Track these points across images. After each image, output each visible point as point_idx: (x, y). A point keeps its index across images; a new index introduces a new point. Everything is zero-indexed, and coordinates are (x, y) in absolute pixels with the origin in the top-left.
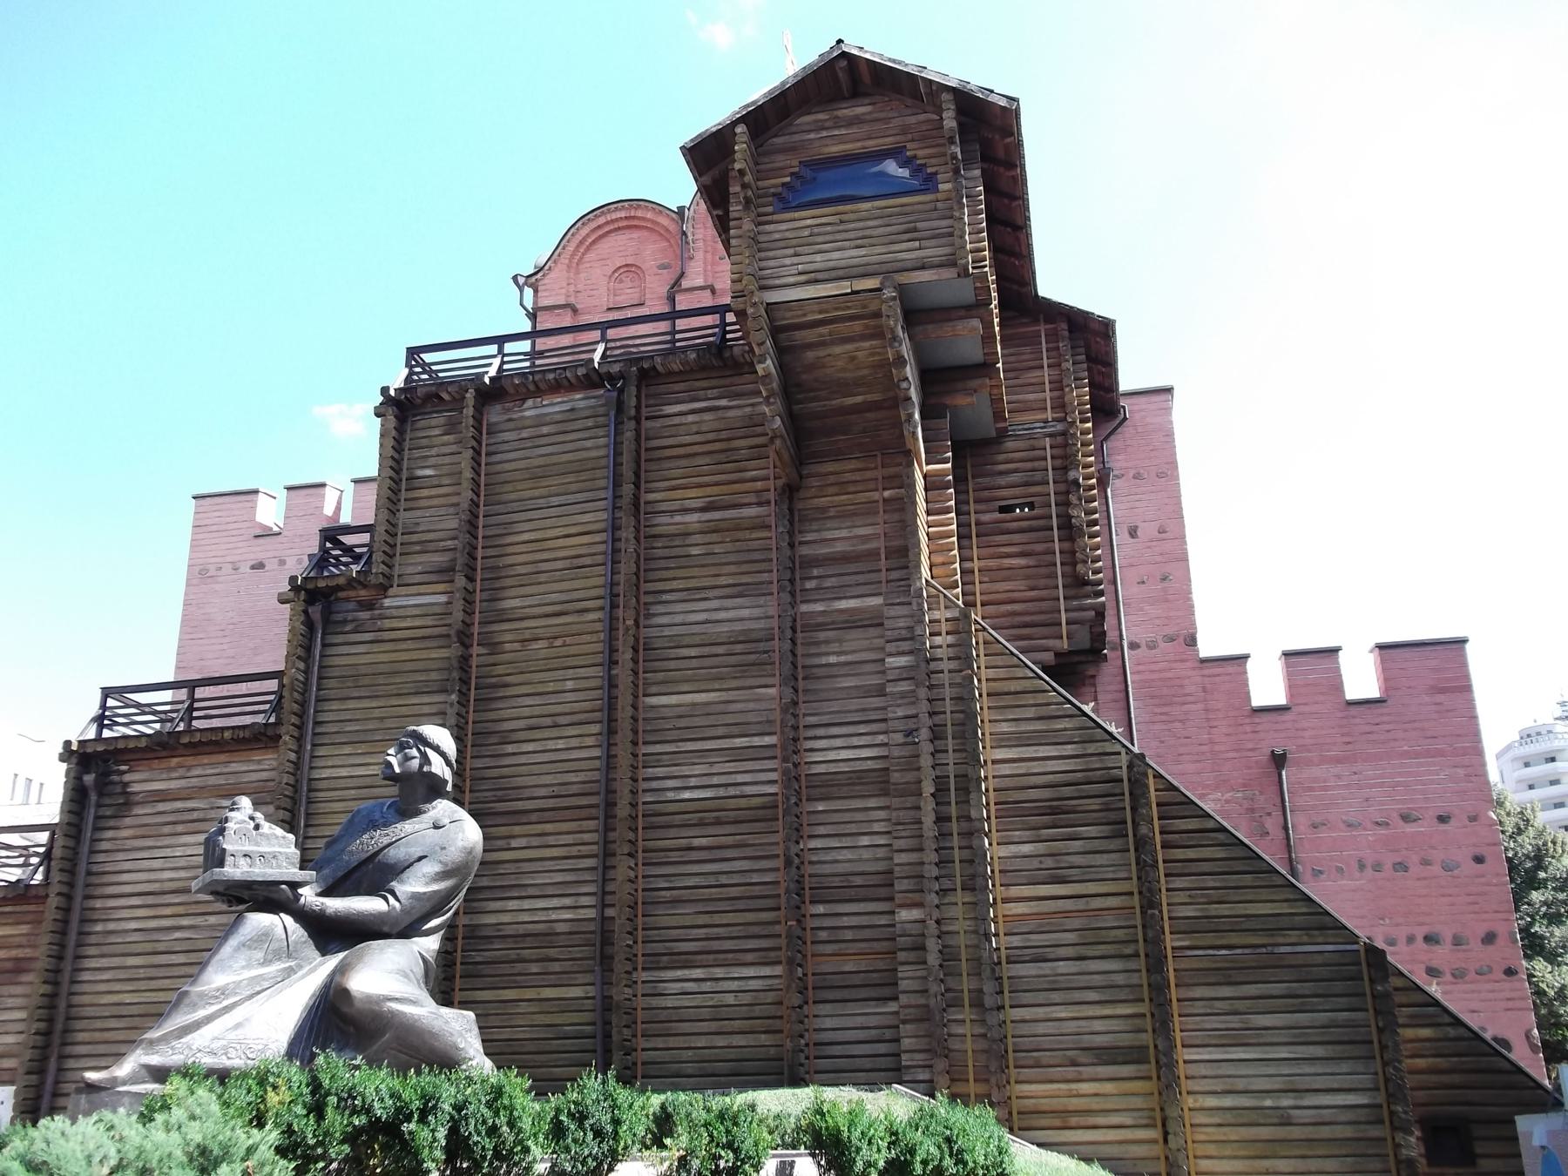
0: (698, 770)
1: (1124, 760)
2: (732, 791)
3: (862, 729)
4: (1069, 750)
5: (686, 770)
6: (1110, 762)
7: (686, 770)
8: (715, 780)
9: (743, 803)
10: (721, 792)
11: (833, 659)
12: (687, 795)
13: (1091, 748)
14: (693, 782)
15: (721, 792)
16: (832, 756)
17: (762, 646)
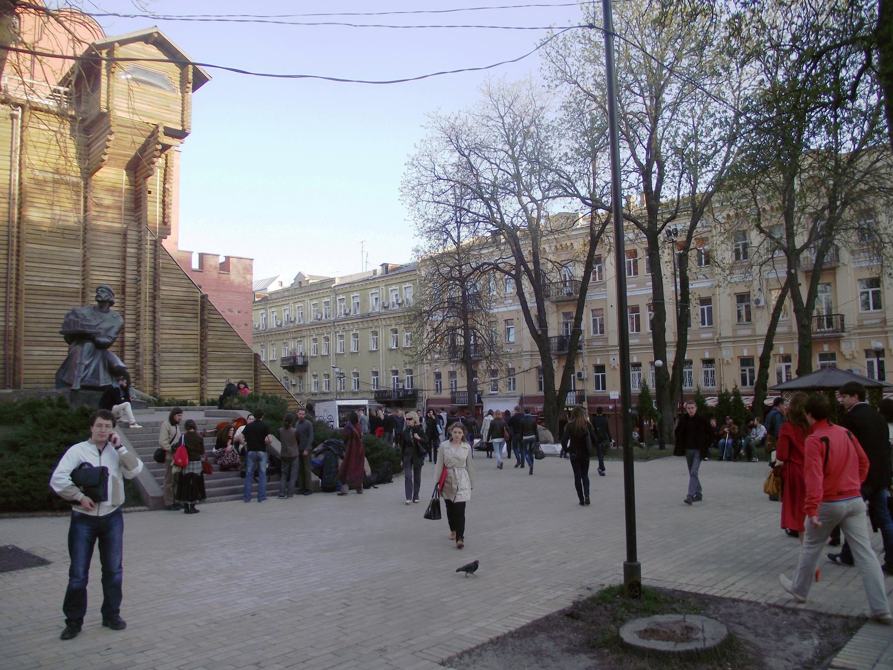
0: (48, 275)
1: (200, 295)
2: (62, 285)
3: (112, 270)
4: (184, 289)
5: (43, 274)
6: (195, 295)
7: (43, 274)
8: (55, 280)
9: (65, 290)
10: (57, 285)
11: (103, 243)
12: (43, 284)
13: (191, 290)
14: (46, 279)
15: (57, 285)
16: (100, 278)
17: (76, 233)
